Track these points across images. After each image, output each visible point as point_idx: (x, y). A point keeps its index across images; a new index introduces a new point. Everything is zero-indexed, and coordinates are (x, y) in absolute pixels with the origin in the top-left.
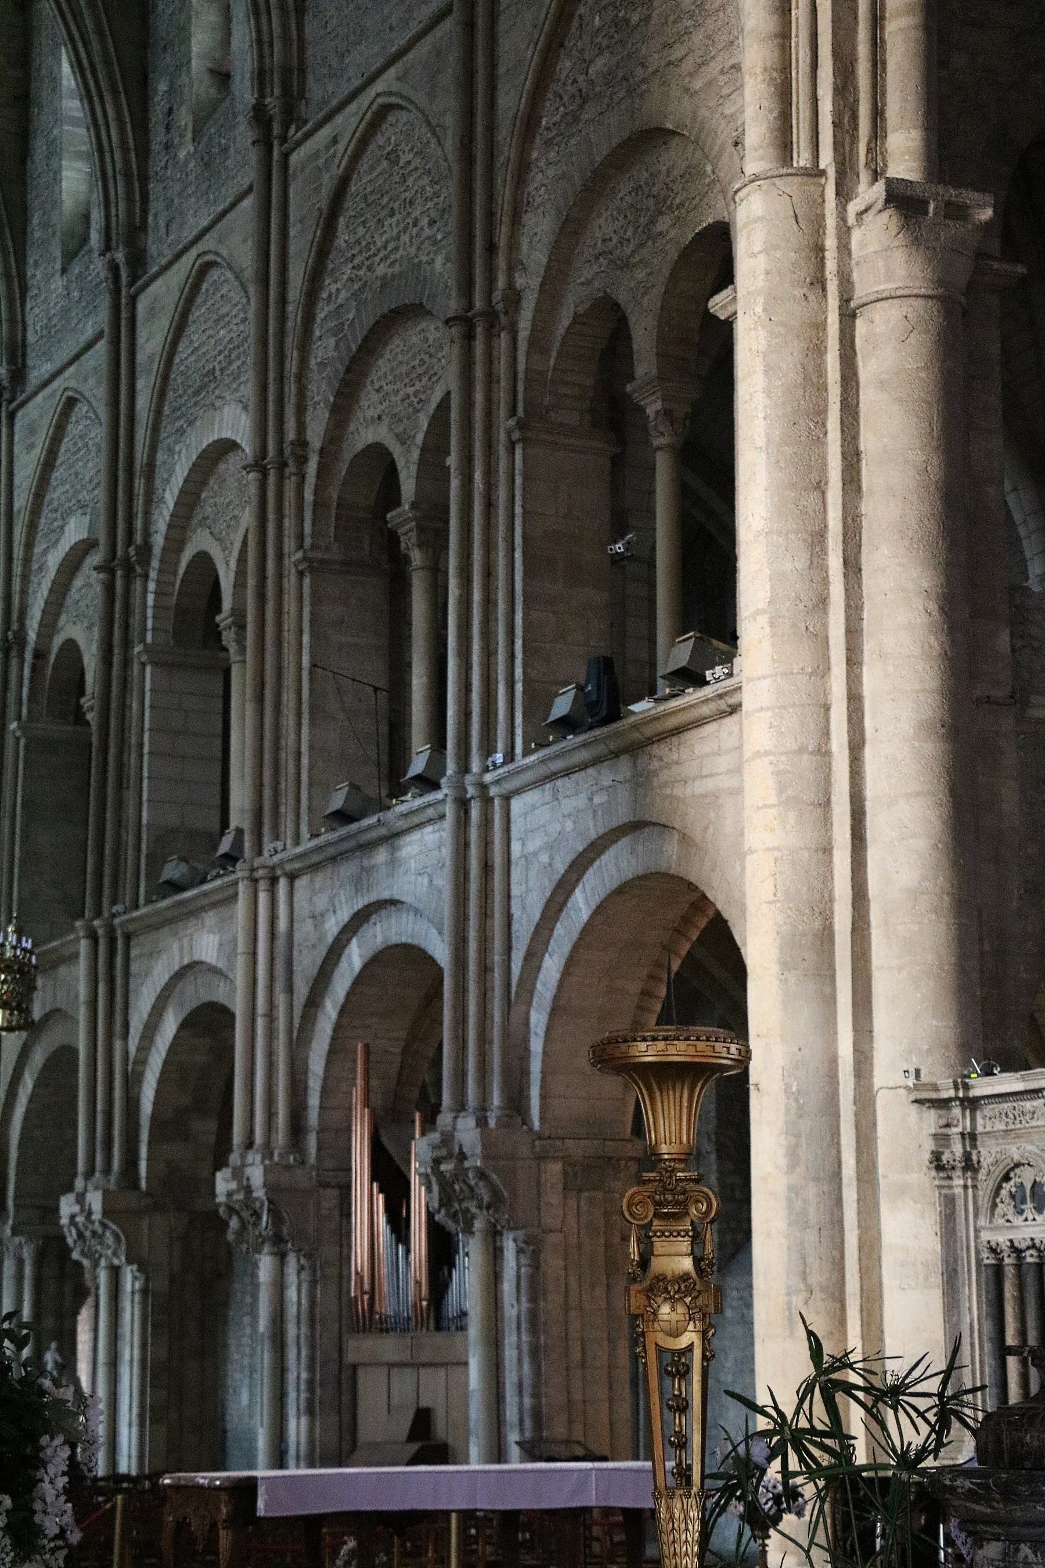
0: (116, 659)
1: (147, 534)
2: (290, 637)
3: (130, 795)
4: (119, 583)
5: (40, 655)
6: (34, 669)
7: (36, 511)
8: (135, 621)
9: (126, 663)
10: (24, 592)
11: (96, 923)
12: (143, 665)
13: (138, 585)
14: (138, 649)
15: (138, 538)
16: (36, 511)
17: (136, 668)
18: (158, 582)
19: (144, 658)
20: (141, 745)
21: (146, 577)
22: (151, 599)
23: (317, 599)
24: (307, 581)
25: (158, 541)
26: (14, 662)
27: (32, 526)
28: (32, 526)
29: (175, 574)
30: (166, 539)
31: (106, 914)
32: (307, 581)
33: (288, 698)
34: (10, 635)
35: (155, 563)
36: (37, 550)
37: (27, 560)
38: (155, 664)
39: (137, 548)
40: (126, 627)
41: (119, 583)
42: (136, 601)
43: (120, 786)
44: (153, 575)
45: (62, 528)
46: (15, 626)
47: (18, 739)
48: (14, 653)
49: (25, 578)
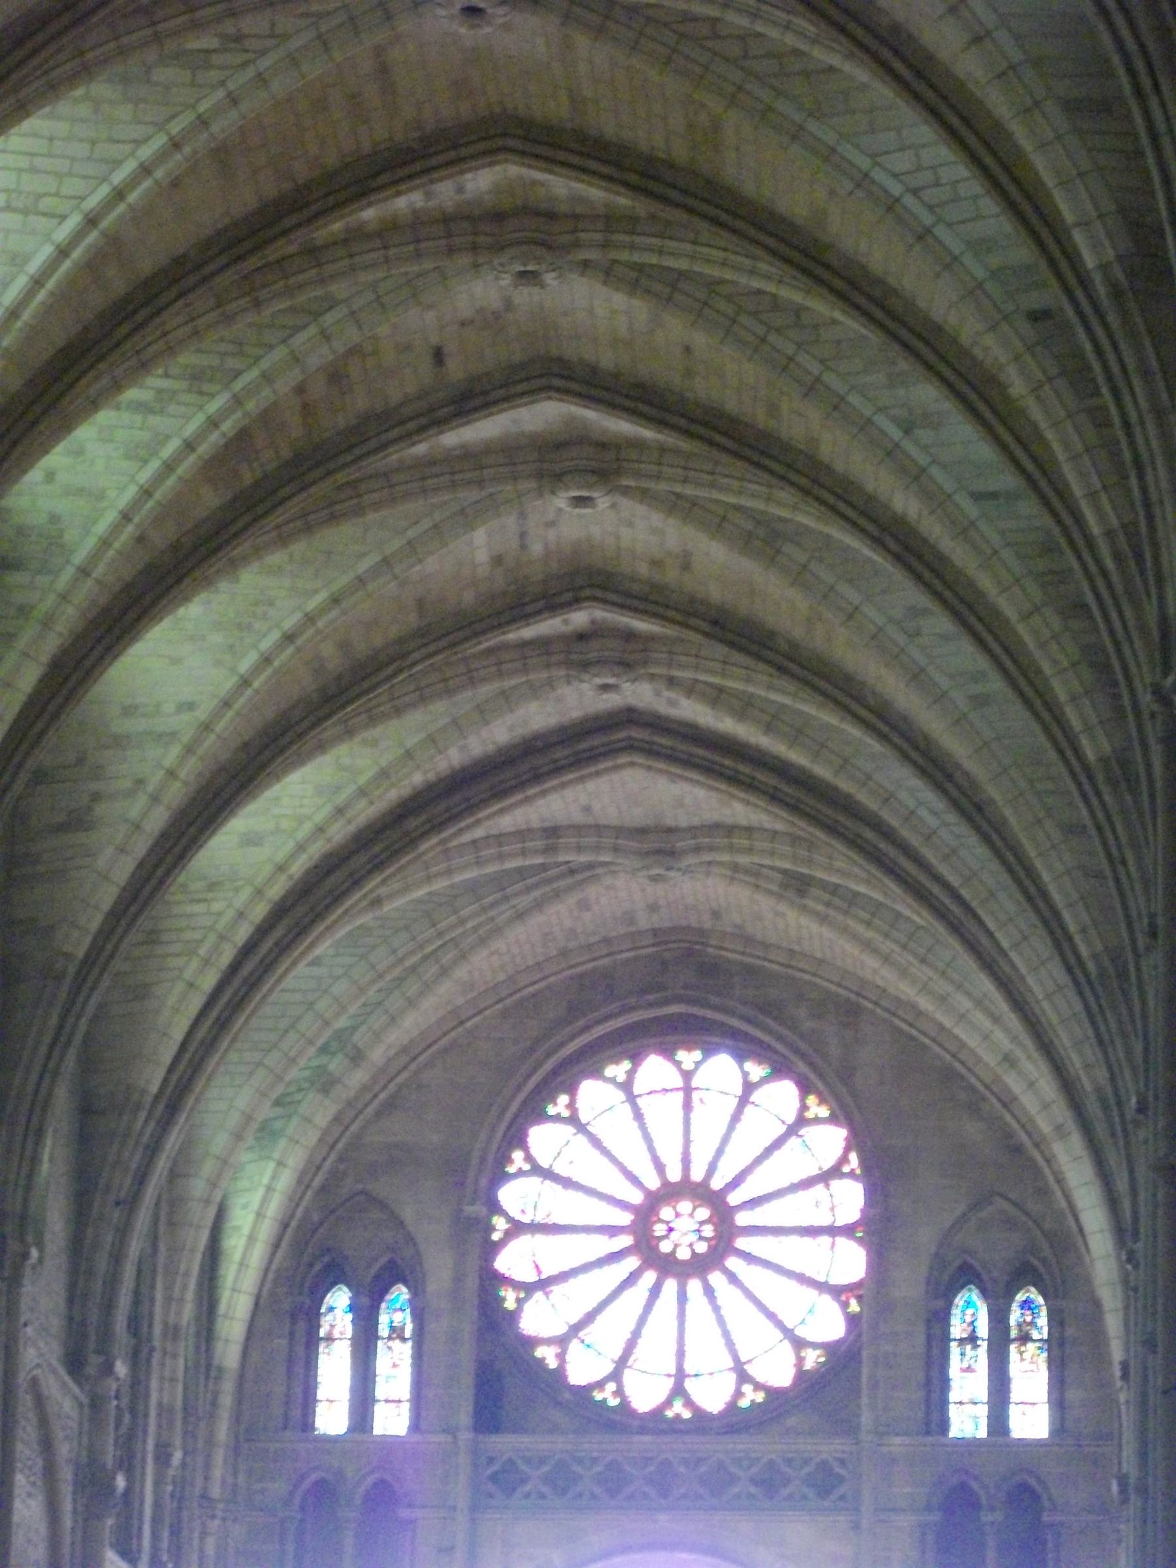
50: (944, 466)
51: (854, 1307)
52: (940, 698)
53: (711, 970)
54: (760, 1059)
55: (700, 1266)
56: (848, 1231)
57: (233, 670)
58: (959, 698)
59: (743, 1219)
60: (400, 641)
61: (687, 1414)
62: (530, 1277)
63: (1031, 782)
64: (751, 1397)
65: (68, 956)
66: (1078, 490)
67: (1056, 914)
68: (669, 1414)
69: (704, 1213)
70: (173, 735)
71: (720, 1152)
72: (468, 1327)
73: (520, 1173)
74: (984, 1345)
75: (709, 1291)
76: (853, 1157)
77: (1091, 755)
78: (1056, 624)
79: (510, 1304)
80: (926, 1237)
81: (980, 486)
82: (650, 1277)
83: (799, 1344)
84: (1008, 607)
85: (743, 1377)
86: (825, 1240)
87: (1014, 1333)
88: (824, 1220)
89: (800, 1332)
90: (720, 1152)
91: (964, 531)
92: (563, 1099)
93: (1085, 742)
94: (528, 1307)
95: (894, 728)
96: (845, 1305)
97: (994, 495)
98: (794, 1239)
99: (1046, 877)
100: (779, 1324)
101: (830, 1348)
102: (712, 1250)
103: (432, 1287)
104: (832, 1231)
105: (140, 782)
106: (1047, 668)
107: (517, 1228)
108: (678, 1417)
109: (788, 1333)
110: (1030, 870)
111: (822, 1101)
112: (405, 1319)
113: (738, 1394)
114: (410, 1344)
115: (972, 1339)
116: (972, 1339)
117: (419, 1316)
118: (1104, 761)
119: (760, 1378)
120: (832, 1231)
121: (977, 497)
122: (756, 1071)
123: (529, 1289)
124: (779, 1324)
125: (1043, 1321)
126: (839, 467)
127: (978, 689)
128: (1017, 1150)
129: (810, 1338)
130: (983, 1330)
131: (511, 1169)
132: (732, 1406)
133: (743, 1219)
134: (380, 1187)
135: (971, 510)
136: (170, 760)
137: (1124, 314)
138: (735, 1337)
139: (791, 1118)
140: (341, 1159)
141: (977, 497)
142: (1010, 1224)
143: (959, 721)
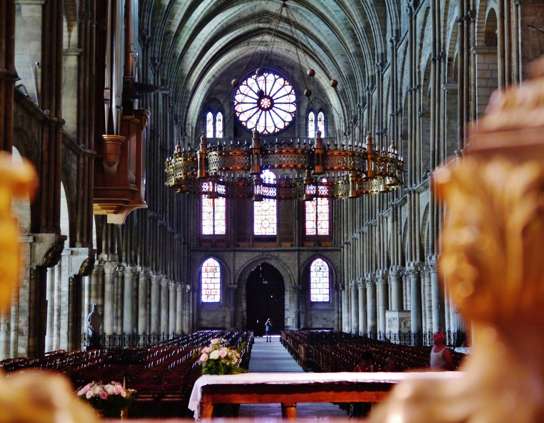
0: (465, 53)
1: (474, 6)
2: (513, 31)
3: (472, 103)
4: (465, 25)
5: (450, 60)
6: (449, 65)
7: (446, 9)
8: (471, 39)
9: (469, 55)
10: (444, 38)
11: (461, 151)
12: (475, 55)
13: (472, 25)
14: (472, 48)
15: (471, 8)
16: (446, 9)
17: (472, 56)
18: (478, 23)
19: (474, 52)
20: (475, 85)
21: (474, 22)
22: (476, 29)
23: (523, 15)
24: (519, 8)
25: (478, 8)
26: (442, 64)
27: (446, 14)
28: (446, 14)
29: (484, 19)
30: (480, 6)
31: (465, 147)
32: (519, 8)
33: (514, 55)
34: (440, 54)
35: (477, 16)
36: (448, 22)
37: (445, 26)
38: (478, 53)
39: (471, 11)
40: (468, 41)
41: (465, 25)
42: (471, 31)
43: (468, 101)
44: (477, 21)
45: (454, 12)
46: (442, 51)
47: (444, 90)
48: (442, 60)
49: (445, 33)
50: (330, 6)
51: (293, 116)
52: (322, 34)
53: (270, 61)
54: (278, 74)
55: (268, 109)
56: (292, 103)
57: (210, 28)
58: (325, 35)
59: (275, 101)
60: (235, 22)
61: (267, 133)
62: (241, 111)
63: (336, 48)
64: (277, 130)
65: (185, 75)
66: (357, 21)
67: (340, 68)
68: (264, 133)
69: (269, 100)
70: (201, 39)
71: (271, 90)
72: (232, 120)
73: (239, 94)
74: (314, 121)
75: (270, 113)
76: (293, 91)
77: (351, 52)
78: (346, 31)
79: (238, 115)
80: (305, 104)
81: (335, 9)
82: (260, 111)
83: (285, 122)
84: (339, 29)
85: (276, 127)
86: (289, 105)
87: (319, 119)
88: (288, 101)
89: (285, 120)
90: (271, 90)
91: (333, 17)
92: (245, 81)
93: (350, 50)
94: (241, 116)
95: (314, 38)
96: (292, 115)
97: (337, 11)
98: (283, 105)
99: (338, 63)
100: (281, 118)
101: (289, 122)
102: (270, 106)
103: (226, 113)
104: (289, 103)
105: (195, 46)
106: (345, 38)
107: (238, 103)
108: (265, 134)
109: (283, 120)
110: (335, 61)
111: (288, 82)
112: (221, 118)
113: (275, 130)
114: (222, 122)
115: (312, 120)
116: (312, 120)
117: (224, 118)
118: (353, 53)
119: (278, 127)
120: (289, 103)
121: (335, 11)
122: (277, 77)
123: (241, 113)
124: (281, 118)
125: (323, 117)
126: (312, 4)
127: (328, 33)
128: (319, 91)
129: (287, 121)
130: (314, 119)
131: (237, 93)
132: (274, 132)
133: (275, 101)
134: (217, 97)
135: (334, 13)
136: (200, 43)
137: (373, 8)
138: (274, 121)
139: (283, 85)
140: (210, 92)
141: (335, 11)
142: (319, 103)
143: (325, 38)
